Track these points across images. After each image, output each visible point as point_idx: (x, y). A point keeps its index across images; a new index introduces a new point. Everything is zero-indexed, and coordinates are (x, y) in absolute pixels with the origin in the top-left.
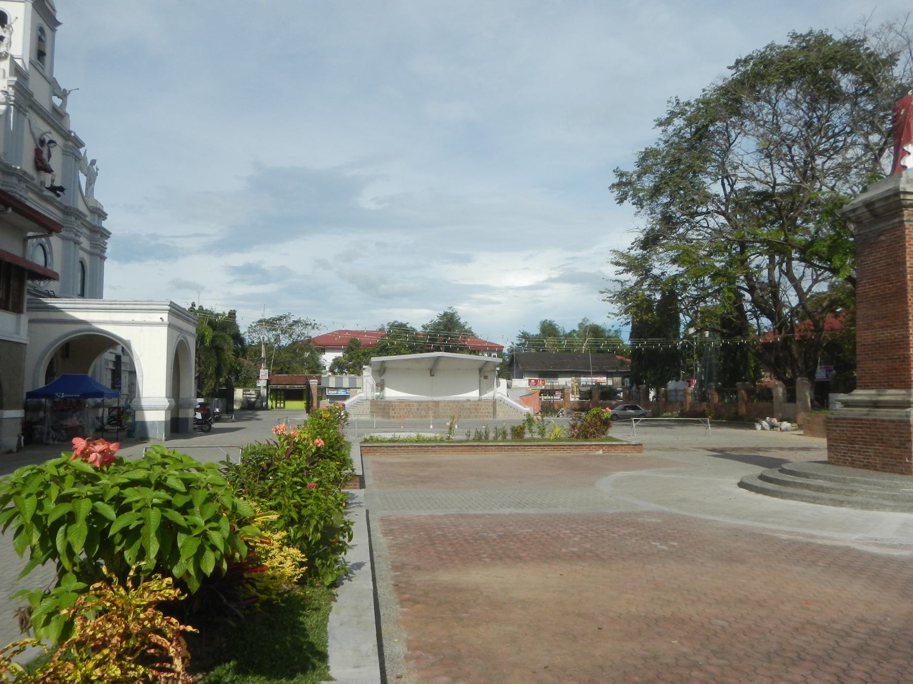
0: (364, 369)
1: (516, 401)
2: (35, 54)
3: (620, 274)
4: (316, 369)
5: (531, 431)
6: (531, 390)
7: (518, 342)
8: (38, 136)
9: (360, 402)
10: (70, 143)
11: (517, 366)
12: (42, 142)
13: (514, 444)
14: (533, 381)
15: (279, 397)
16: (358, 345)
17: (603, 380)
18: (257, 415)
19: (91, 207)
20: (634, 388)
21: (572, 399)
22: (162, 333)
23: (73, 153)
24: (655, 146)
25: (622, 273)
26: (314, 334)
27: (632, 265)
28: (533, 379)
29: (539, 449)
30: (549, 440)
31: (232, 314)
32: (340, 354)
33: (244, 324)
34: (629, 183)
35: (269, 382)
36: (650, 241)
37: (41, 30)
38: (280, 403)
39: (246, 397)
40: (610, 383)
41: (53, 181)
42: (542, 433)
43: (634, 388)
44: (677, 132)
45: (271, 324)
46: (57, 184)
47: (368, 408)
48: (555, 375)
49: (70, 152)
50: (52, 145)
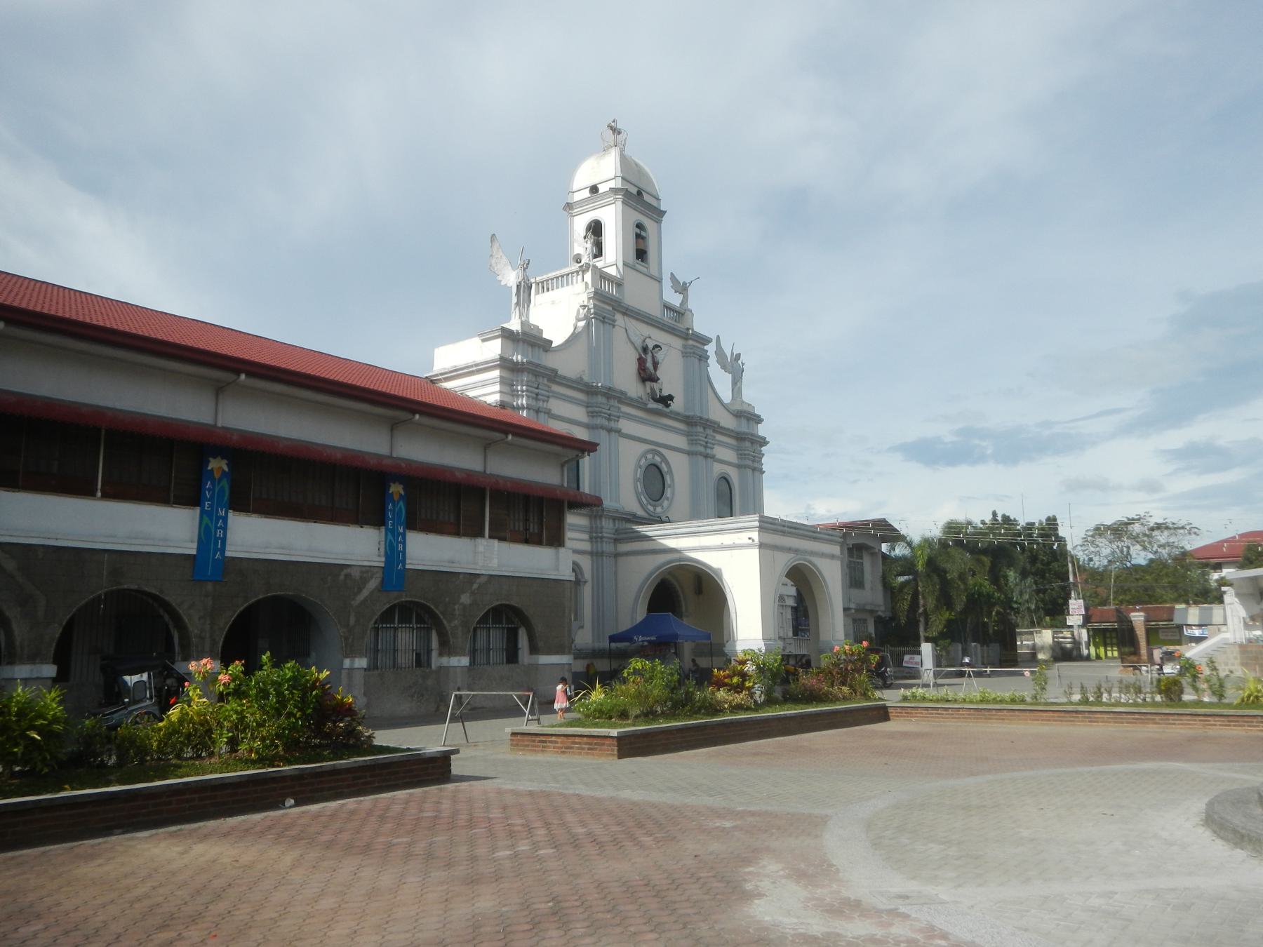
2: (632, 254)
5: (1196, 689)
8: (639, 343)
9: (1223, 647)
10: (691, 342)
12: (645, 349)
13: (1167, 711)
15: (1108, 641)
19: (734, 411)
22: (753, 557)
23: (694, 353)
29: (1219, 721)
30: (1229, 706)
31: (1052, 523)
33: (1072, 534)
35: (1087, 619)
38: (1112, 651)
39: (1058, 642)
42: (1219, 691)
45: (1118, 530)
46: (665, 393)
47: (1236, 658)
49: (690, 353)
50: (657, 349)
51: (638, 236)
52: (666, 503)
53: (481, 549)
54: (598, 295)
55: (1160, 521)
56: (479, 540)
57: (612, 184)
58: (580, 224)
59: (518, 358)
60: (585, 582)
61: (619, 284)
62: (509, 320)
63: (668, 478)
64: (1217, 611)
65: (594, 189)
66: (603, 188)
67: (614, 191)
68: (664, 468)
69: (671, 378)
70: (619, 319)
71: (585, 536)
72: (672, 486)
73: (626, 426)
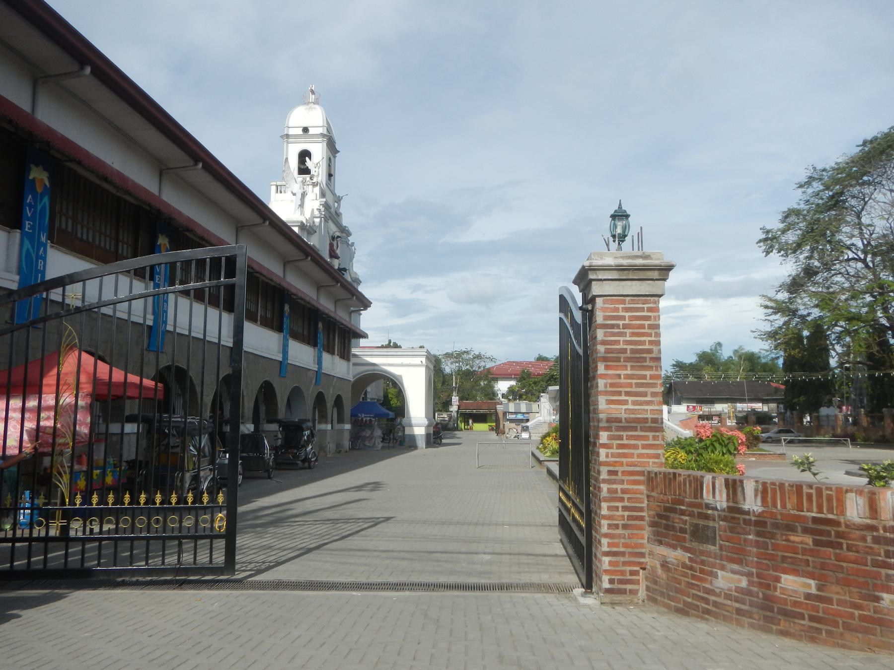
0: (542, 396)
1: (676, 425)
3: (769, 316)
4: (491, 394)
6: (689, 415)
7: (673, 370)
11: (676, 393)
14: (691, 407)
16: (529, 375)
17: (759, 406)
18: (455, 434)
20: (788, 413)
21: (729, 424)
22: (422, 372)
24: (796, 206)
25: (771, 315)
26: (489, 365)
27: (779, 308)
28: (691, 405)
32: (513, 383)
34: (774, 238)
36: (795, 286)
37: (330, 159)
40: (766, 409)
41: (339, 264)
43: (788, 413)
44: (817, 194)
48: (712, 401)
50: (339, 239)
55: (477, 353)
57: (320, 131)
58: (293, 152)
64: (534, 406)
65: (306, 130)
66: (312, 131)
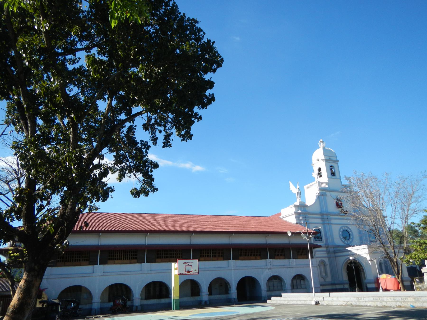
12: (337, 199)
51: (331, 169)
52: (351, 240)
53: (291, 261)
54: (320, 189)
56: (290, 260)
59: (299, 211)
60: (327, 265)
61: (327, 184)
62: (296, 201)
63: (351, 233)
67: (322, 160)
68: (349, 230)
69: (347, 206)
70: (328, 193)
71: (326, 253)
72: (353, 235)
73: (333, 221)
